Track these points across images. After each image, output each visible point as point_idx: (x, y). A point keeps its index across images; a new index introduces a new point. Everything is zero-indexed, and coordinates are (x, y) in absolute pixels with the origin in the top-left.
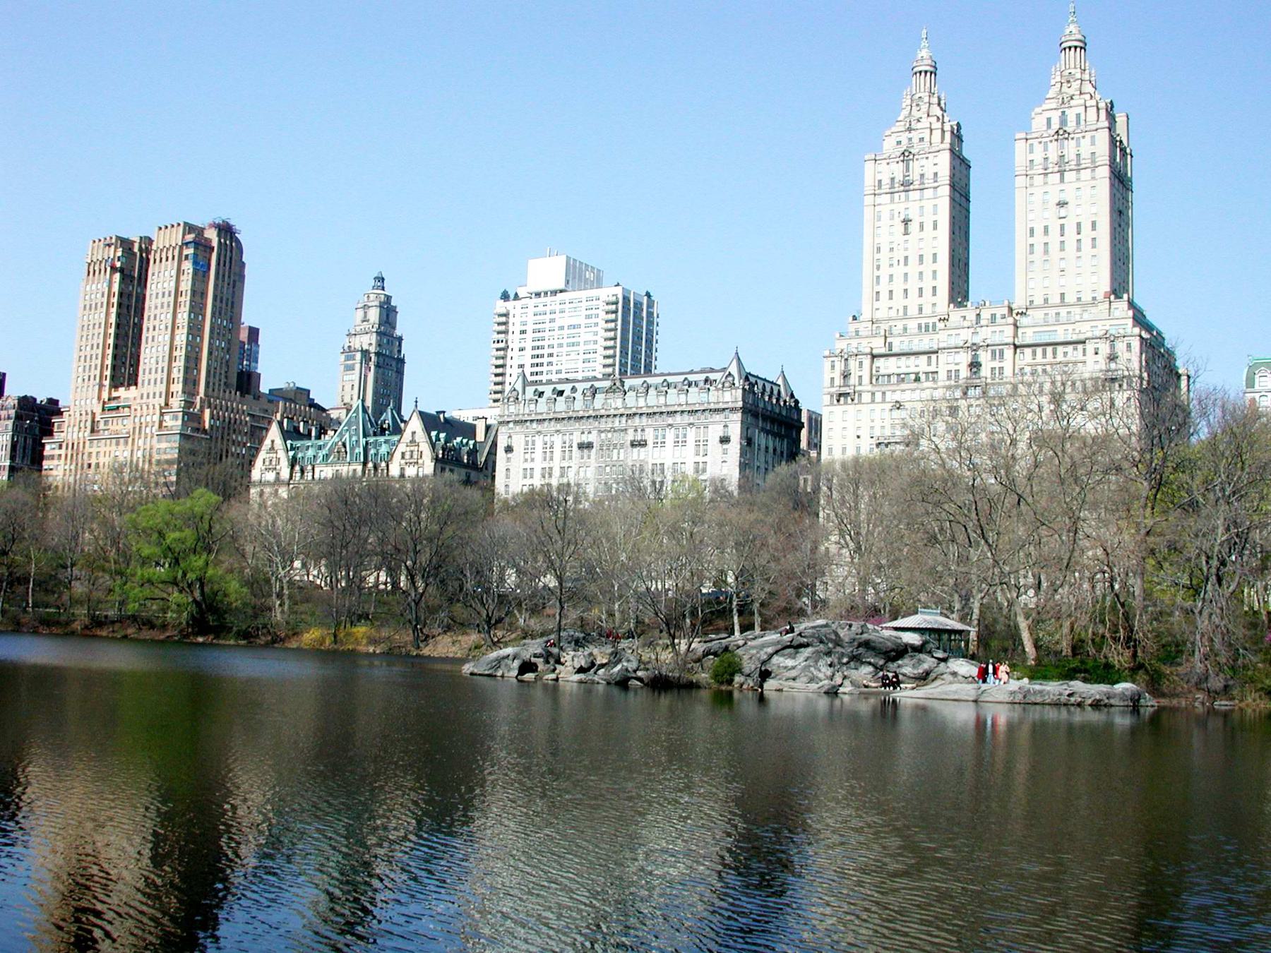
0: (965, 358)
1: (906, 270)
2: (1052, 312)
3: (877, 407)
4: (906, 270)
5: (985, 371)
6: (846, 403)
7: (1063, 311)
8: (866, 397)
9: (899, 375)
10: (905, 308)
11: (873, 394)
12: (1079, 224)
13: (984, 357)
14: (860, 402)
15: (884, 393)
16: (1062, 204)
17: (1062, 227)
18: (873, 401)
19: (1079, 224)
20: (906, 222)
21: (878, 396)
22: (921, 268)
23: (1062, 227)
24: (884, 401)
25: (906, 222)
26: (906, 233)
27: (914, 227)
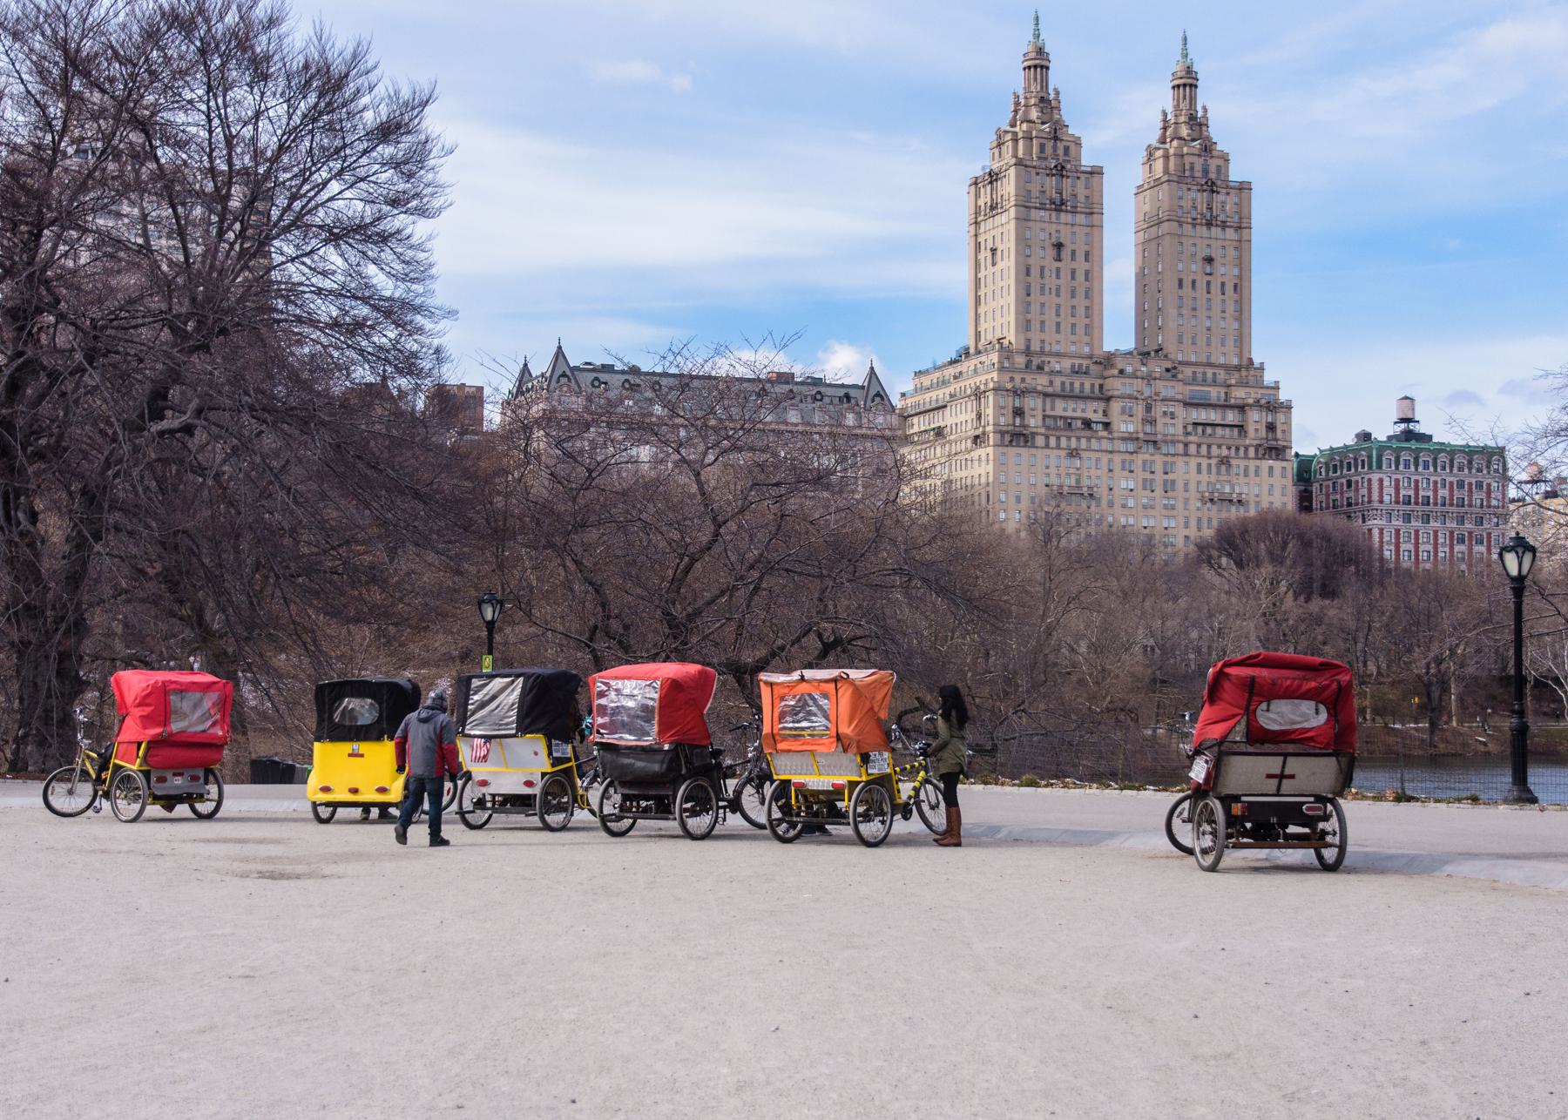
0: (1139, 410)
1: (1058, 300)
2: (1200, 370)
4: (1058, 300)
5: (1160, 427)
6: (1018, 446)
7: (1210, 372)
8: (1040, 441)
9: (1065, 418)
11: (1047, 437)
12: (1223, 284)
13: (1159, 410)
14: (1033, 446)
15: (1058, 438)
16: (1209, 260)
17: (1208, 283)
18: (1047, 446)
19: (1223, 284)
20: (1059, 246)
21: (1053, 441)
22: (1075, 302)
23: (1208, 283)
24: (1058, 447)
25: (1059, 246)
26: (1058, 259)
27: (1066, 254)
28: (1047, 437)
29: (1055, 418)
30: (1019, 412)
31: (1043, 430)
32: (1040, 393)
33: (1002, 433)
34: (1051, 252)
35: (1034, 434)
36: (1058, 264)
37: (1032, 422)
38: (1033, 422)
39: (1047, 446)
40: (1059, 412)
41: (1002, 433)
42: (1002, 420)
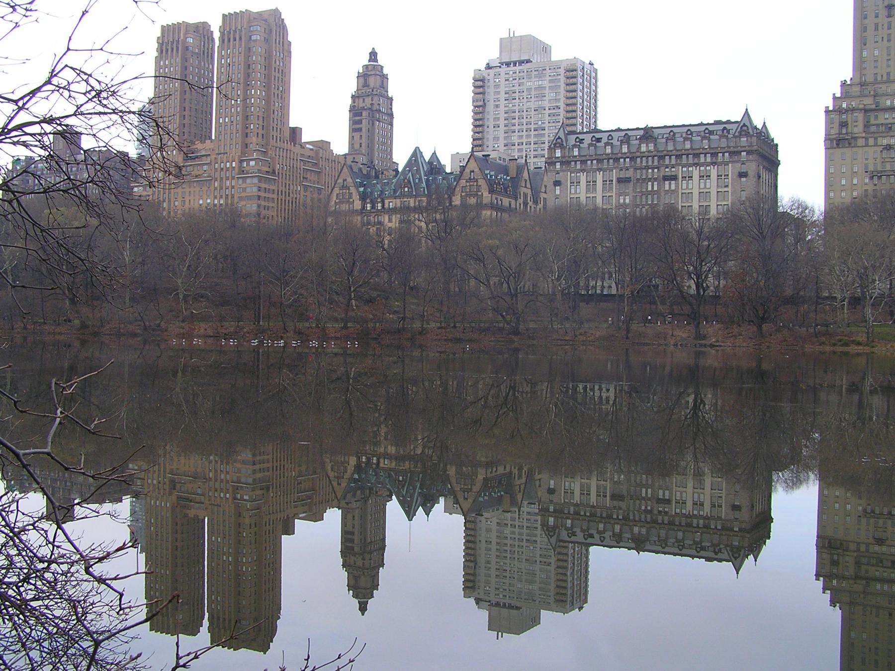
1: (889, 44)
3: (871, 150)
4: (889, 44)
8: (861, 142)
10: (888, 74)
11: (867, 139)
14: (856, 146)
15: (876, 139)
21: (871, 141)
24: (876, 145)
28: (867, 139)
29: (877, 125)
30: (843, 124)
31: (864, 135)
32: (861, 110)
33: (832, 140)
34: (883, 13)
35: (855, 138)
36: (890, 19)
37: (856, 130)
38: (858, 129)
39: (867, 145)
40: (881, 120)
41: (832, 140)
42: (833, 132)
